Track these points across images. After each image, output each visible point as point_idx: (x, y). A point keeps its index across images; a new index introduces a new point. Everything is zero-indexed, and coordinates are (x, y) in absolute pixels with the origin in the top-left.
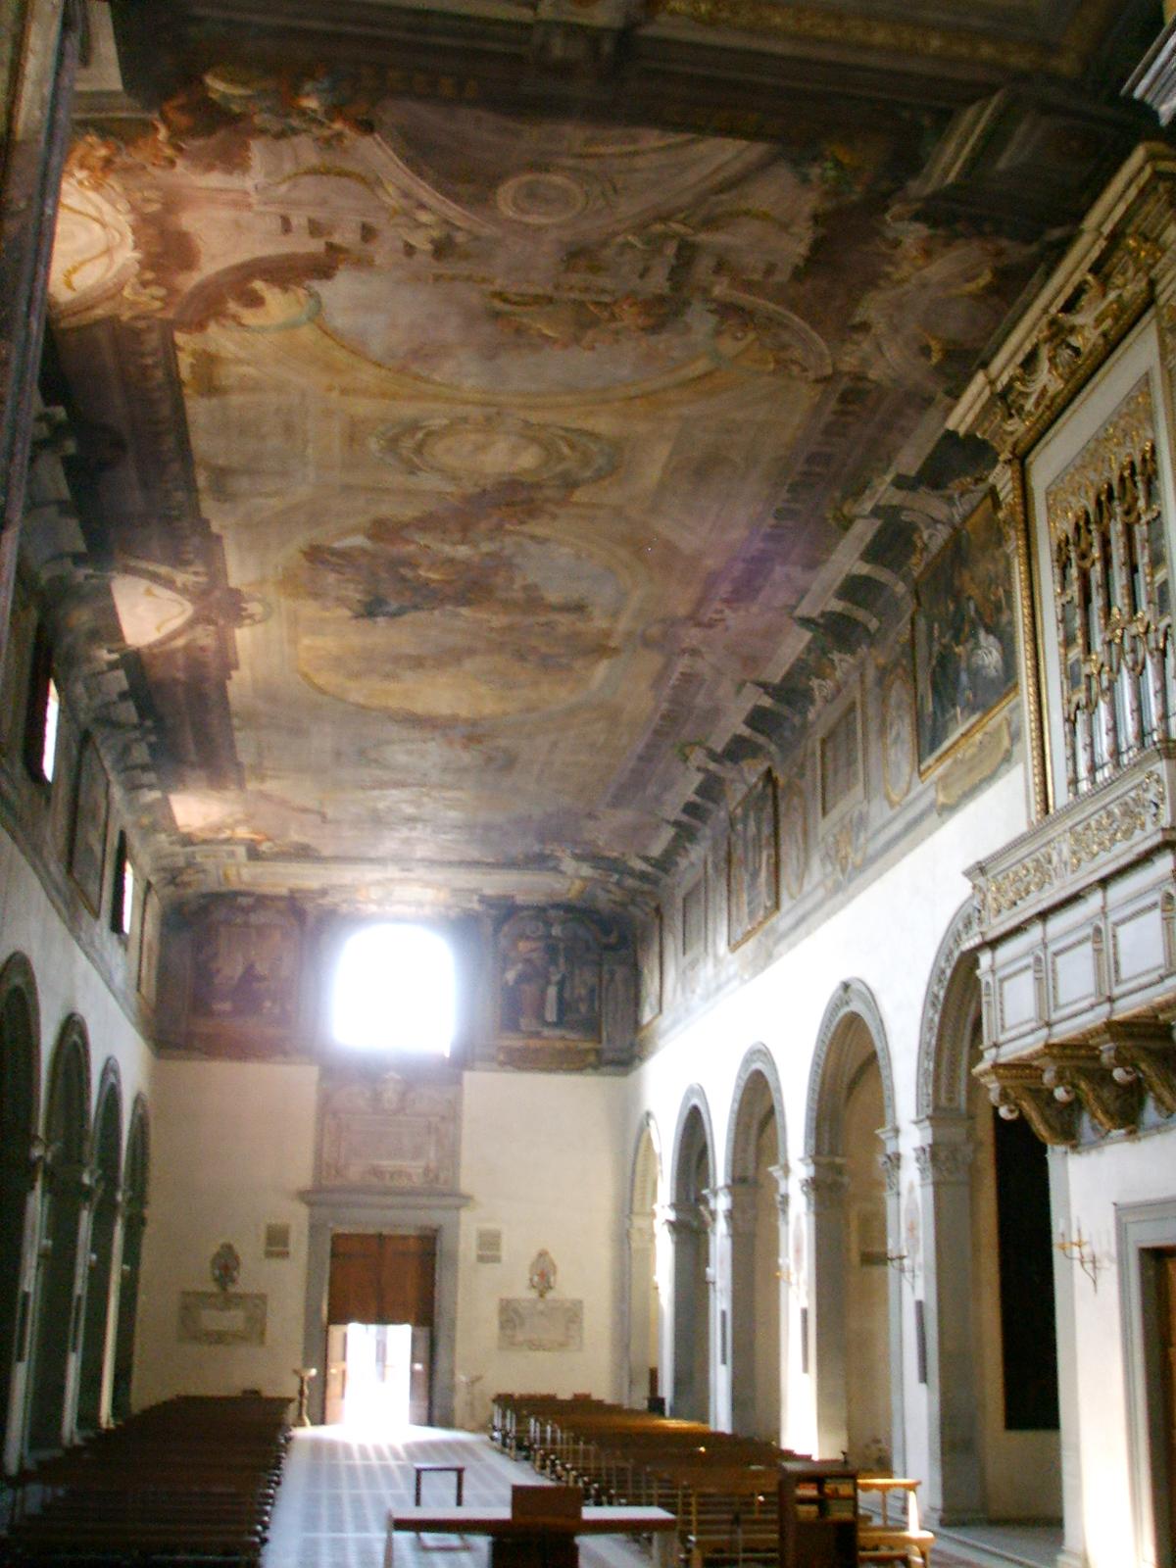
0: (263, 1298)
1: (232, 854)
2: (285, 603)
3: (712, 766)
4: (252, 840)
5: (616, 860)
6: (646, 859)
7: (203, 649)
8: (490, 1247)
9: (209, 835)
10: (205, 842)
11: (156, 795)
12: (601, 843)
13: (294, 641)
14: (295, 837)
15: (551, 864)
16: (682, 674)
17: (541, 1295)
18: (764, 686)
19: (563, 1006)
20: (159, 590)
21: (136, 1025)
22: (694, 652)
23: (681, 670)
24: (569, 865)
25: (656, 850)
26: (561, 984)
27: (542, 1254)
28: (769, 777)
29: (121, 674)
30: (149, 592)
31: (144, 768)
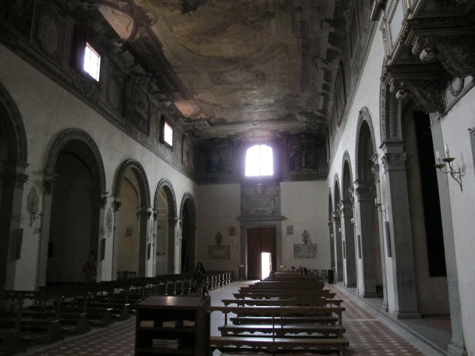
0: (229, 246)
1: (205, 125)
2: (157, 10)
3: (325, 66)
4: (207, 118)
5: (311, 113)
6: (319, 111)
7: (146, 38)
8: (290, 230)
9: (195, 118)
10: (194, 121)
11: (169, 103)
12: (304, 107)
13: (171, 30)
14: (218, 116)
15: (294, 117)
16: (300, 22)
17: (306, 243)
18: (328, 21)
19: (307, 162)
20: (116, 11)
21: (184, 174)
22: (300, 9)
23: (299, 20)
24: (299, 117)
25: (321, 107)
26: (306, 157)
27: (305, 232)
28: (341, 63)
29: (127, 52)
30: (114, 13)
31: (161, 93)
